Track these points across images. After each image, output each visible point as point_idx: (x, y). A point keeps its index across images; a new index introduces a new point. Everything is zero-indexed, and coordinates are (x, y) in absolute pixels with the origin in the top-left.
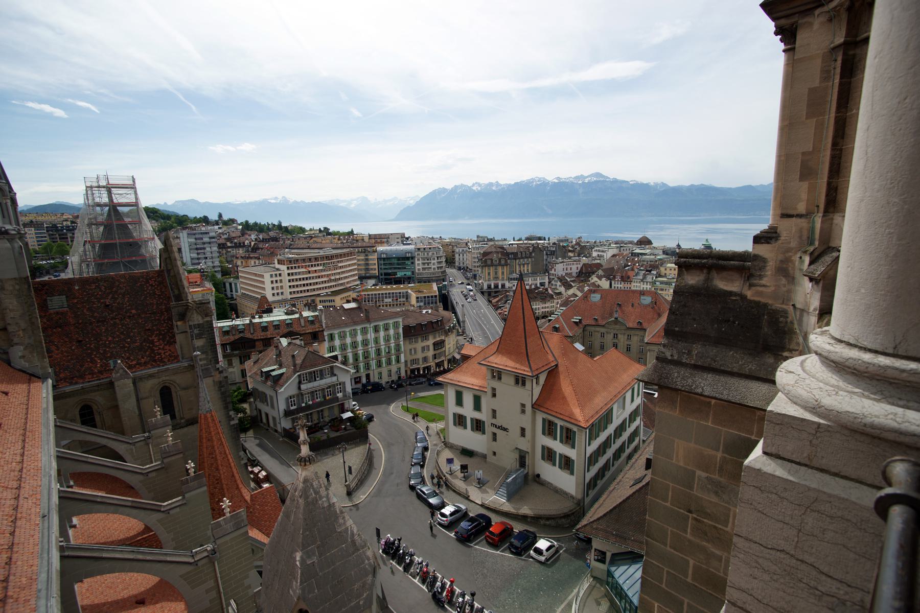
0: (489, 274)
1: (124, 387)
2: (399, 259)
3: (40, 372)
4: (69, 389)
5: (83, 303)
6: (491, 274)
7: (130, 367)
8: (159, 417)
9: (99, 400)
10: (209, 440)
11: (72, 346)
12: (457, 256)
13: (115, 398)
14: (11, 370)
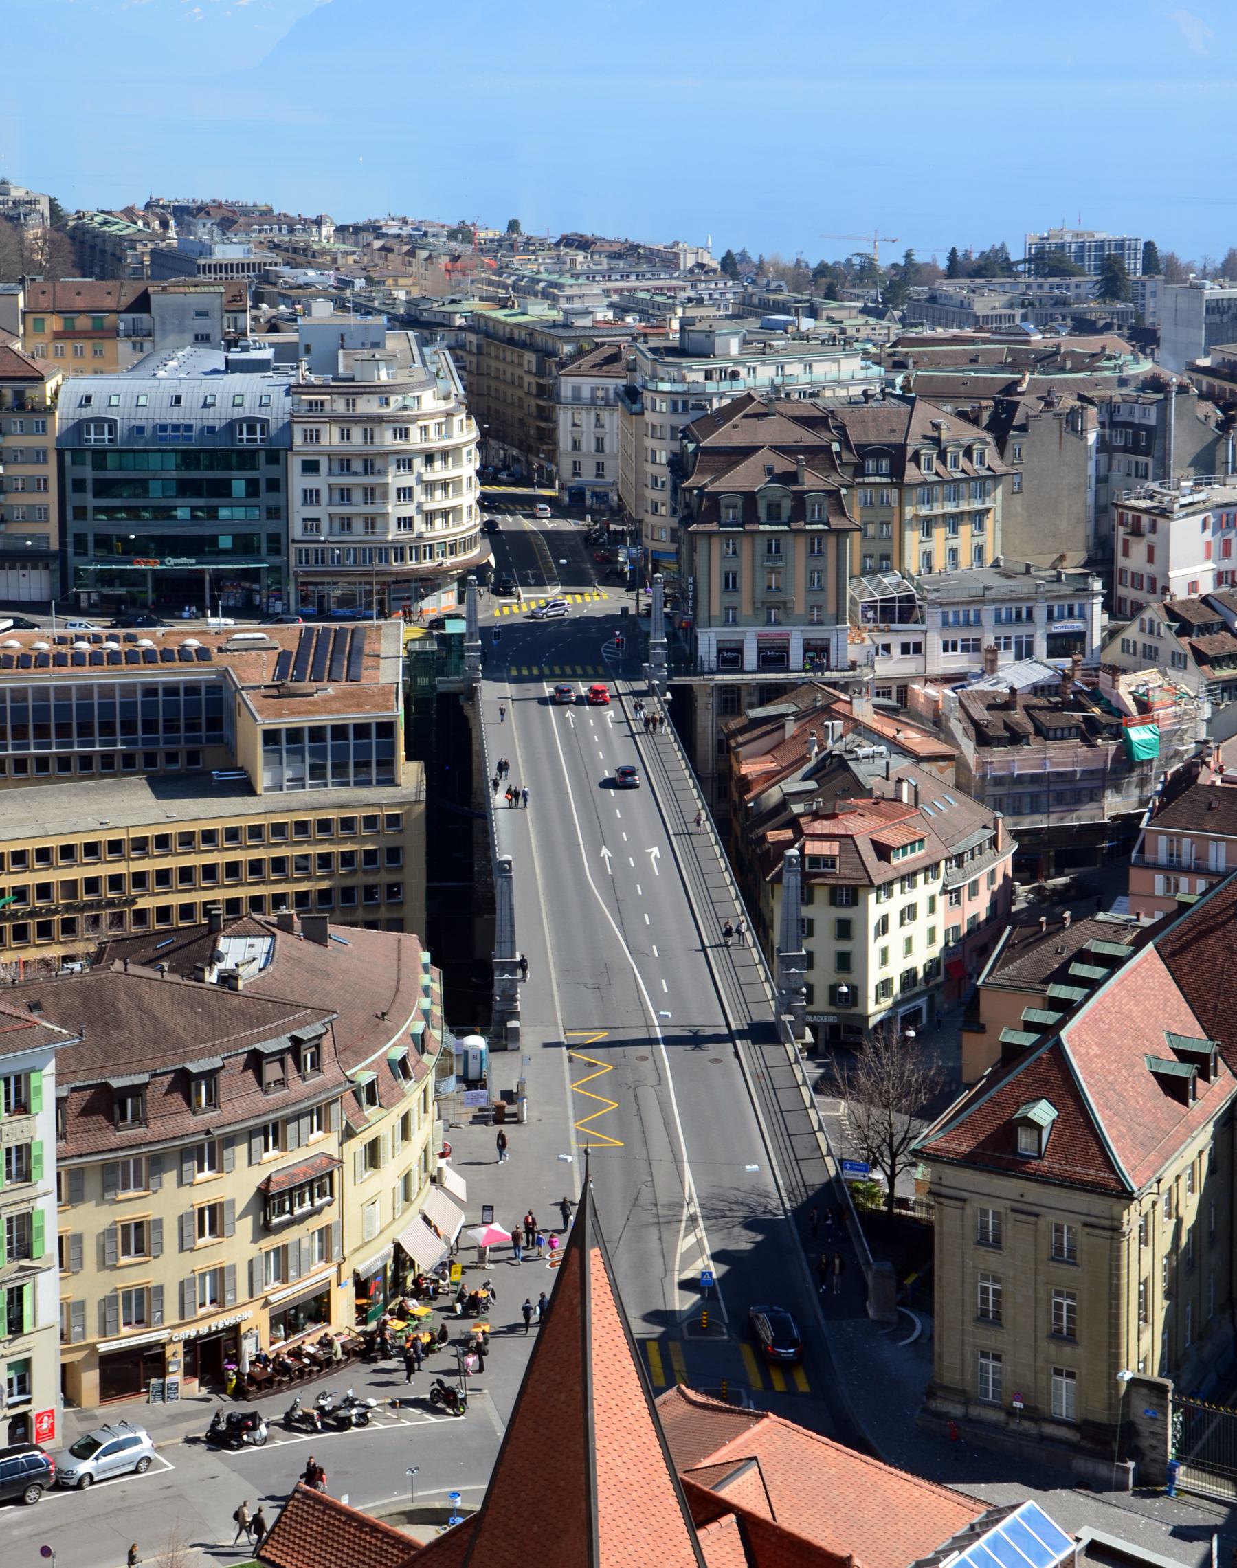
0: (730, 583)
2: (189, 459)
6: (744, 582)
12: (564, 419)
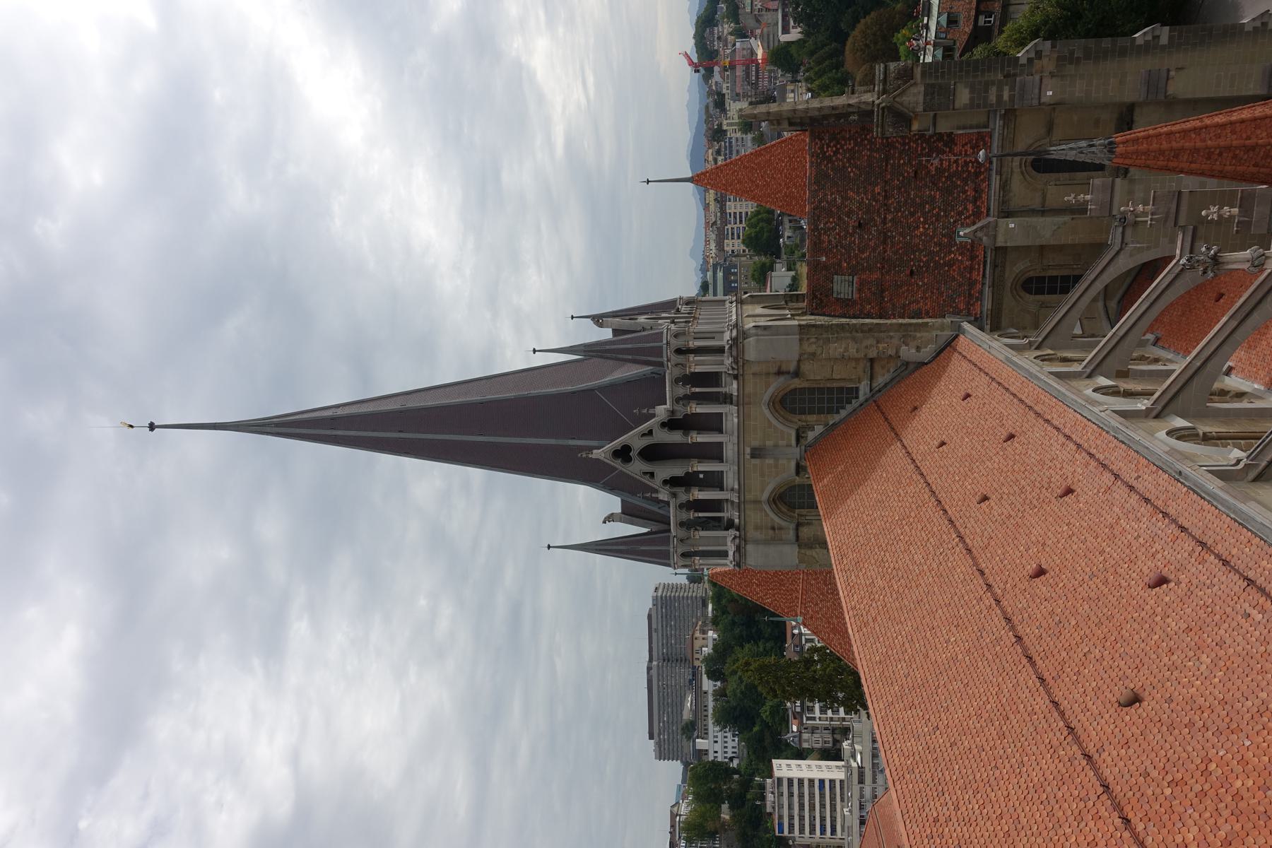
1: (1011, 230)
3: (948, 333)
4: (987, 304)
5: (850, 257)
7: (977, 215)
8: (1088, 197)
9: (1017, 268)
10: (1176, 156)
11: (917, 284)
13: (1028, 248)
14: (934, 365)
